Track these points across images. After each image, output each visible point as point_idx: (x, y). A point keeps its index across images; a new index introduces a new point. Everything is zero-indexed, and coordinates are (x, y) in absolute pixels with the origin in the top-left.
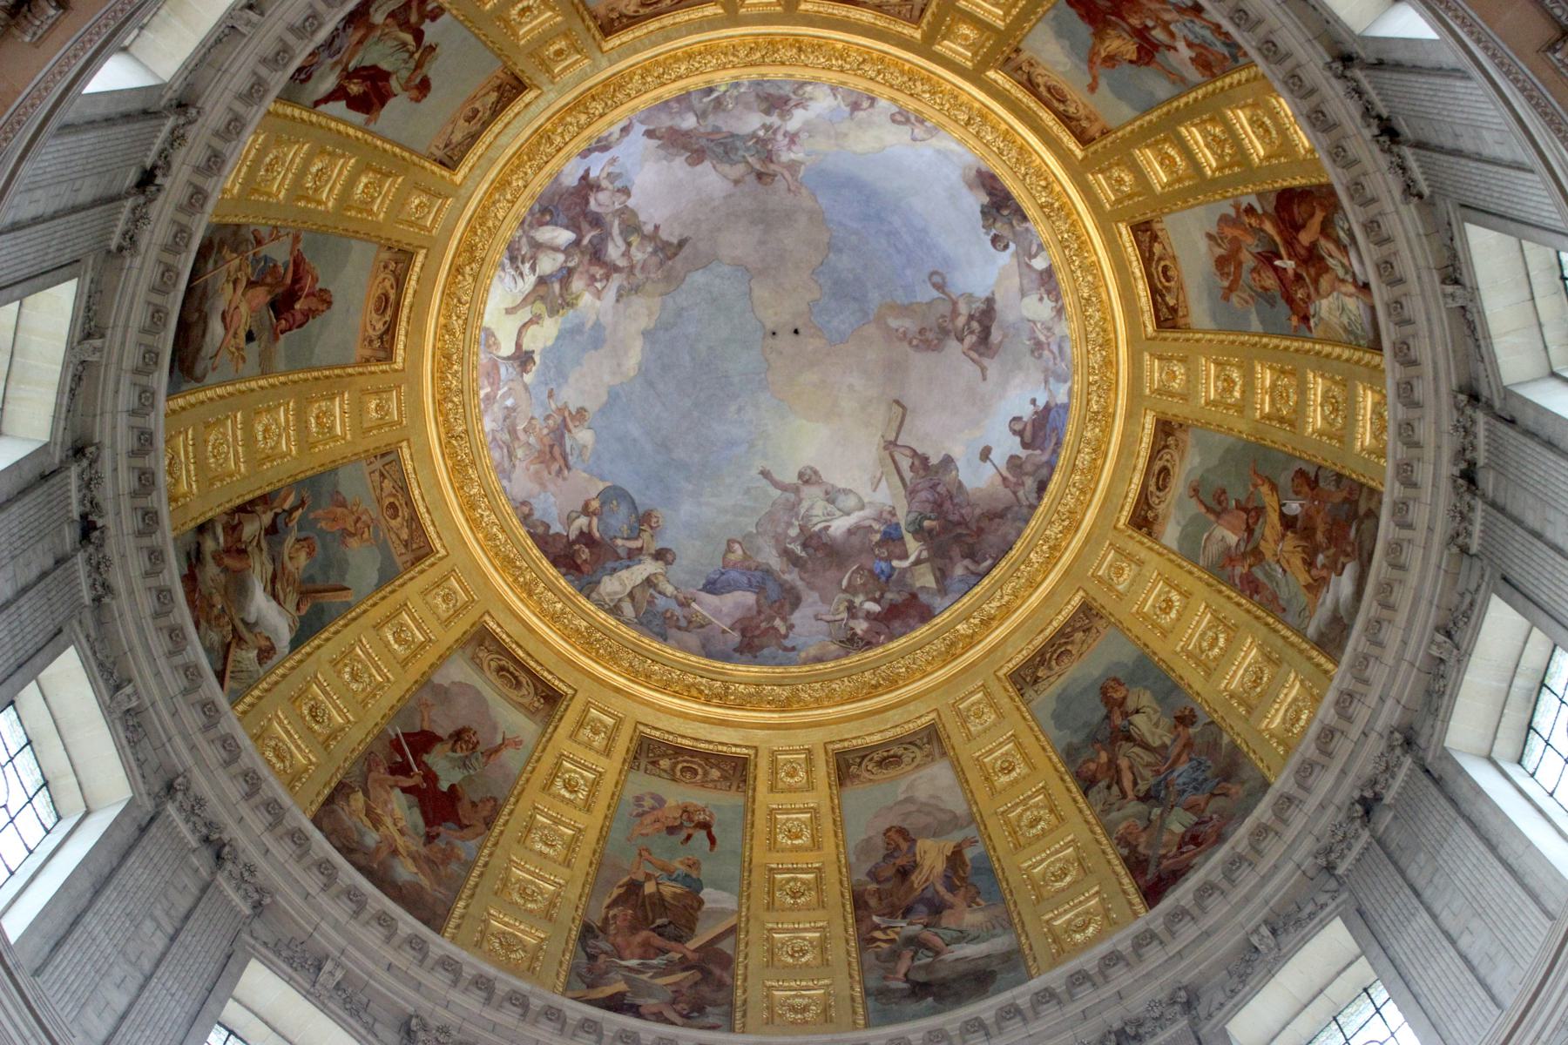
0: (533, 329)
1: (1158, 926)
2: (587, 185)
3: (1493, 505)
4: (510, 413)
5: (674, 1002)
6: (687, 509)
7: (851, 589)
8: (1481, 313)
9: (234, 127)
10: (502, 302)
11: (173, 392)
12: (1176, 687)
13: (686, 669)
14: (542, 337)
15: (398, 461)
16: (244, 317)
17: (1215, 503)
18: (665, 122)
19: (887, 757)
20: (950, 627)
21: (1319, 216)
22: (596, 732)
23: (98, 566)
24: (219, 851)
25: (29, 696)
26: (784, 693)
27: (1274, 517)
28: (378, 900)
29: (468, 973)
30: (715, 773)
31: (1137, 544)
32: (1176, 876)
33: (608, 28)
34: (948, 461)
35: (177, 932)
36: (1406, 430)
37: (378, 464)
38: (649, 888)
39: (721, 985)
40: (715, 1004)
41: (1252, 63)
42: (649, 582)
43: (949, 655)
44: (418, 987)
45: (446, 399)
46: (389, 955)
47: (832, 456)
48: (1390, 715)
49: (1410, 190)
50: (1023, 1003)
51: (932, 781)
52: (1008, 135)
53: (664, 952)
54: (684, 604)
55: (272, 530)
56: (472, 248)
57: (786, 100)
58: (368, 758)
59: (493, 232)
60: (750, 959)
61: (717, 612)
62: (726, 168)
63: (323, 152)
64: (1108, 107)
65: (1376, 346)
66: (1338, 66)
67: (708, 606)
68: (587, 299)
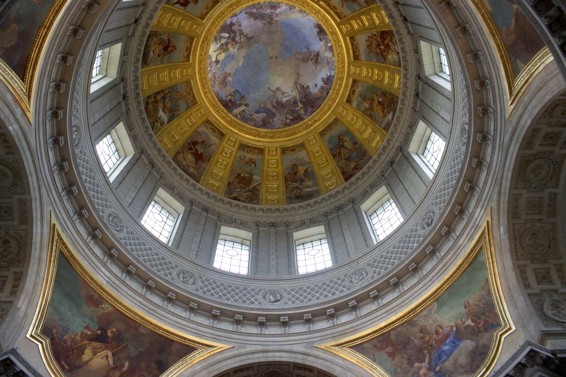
0: (220, 55)
1: (347, 186)
2: (232, 24)
3: (422, 101)
4: (214, 74)
5: (247, 198)
6: (252, 95)
7: (286, 114)
8: (422, 60)
9: (155, 9)
10: (213, 49)
11: (142, 68)
12: (354, 136)
13: (251, 129)
15: (190, 84)
16: (157, 51)
17: (364, 98)
18: (249, 10)
19: (293, 149)
20: (307, 122)
21: (389, 37)
22: (231, 142)
23: (127, 105)
24: (153, 165)
25: (113, 132)
26: (271, 135)
27: (376, 101)
28: (186, 176)
29: (204, 191)
30: (256, 151)
31: (347, 106)
32: (352, 176)
34: (308, 87)
35: (145, 181)
36: (405, 85)
37: (186, 84)
38: (242, 175)
39: (257, 195)
40: (255, 199)
41: (377, 3)
42: (243, 111)
43: (307, 128)
44: (194, 194)
45: (201, 70)
46: (188, 187)
47: (283, 84)
48: (397, 144)
49: (409, 33)
50: (319, 201)
51: (302, 155)
52: (324, 16)
53: (245, 188)
54: (251, 115)
55: (163, 98)
56: (207, 37)
57: (276, 6)
58: (183, 147)
59: (211, 34)
60: (263, 191)
61: (258, 117)
62: (262, 21)
63: (175, 15)
64: (346, 11)
65: (400, 66)
66: (395, 4)
67: (255, 116)
68: (231, 49)
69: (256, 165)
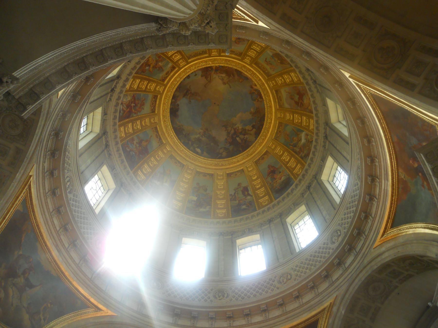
0: (250, 129)
14: (248, 127)
15: (275, 137)
27: (151, 66)
30: (260, 65)
33: (212, 175)
34: (202, 76)
38: (279, 61)
47: (218, 84)
55: (295, 146)
56: (247, 156)
68: (240, 128)
69: (266, 59)
